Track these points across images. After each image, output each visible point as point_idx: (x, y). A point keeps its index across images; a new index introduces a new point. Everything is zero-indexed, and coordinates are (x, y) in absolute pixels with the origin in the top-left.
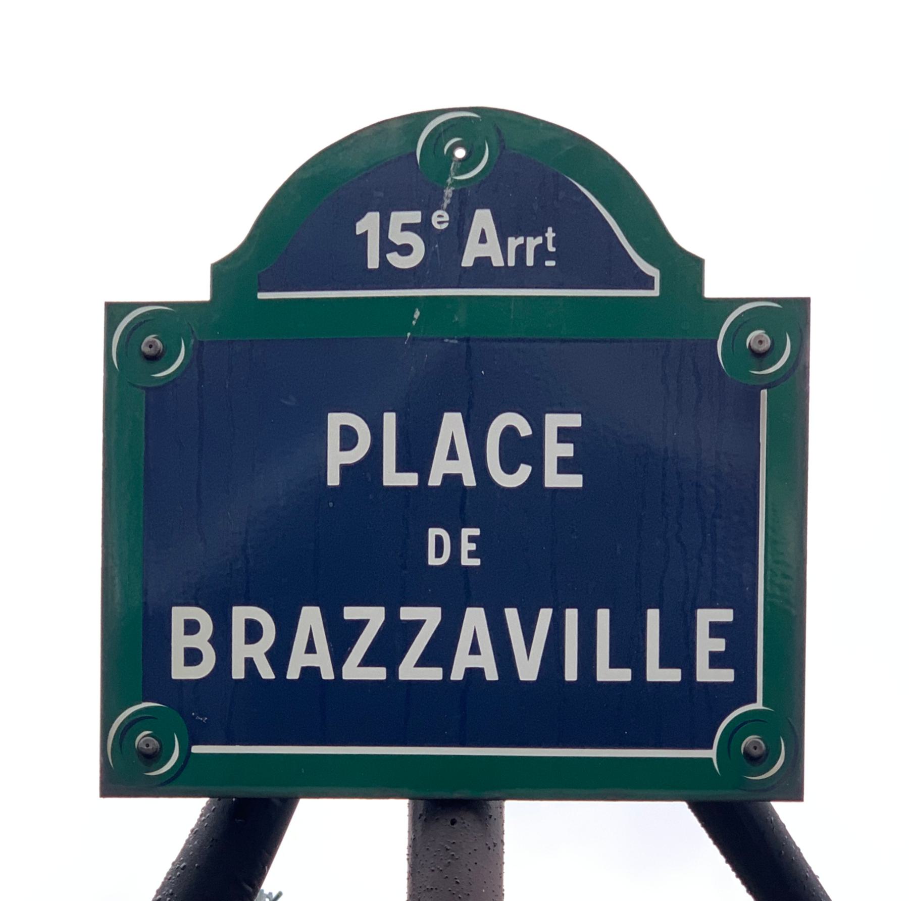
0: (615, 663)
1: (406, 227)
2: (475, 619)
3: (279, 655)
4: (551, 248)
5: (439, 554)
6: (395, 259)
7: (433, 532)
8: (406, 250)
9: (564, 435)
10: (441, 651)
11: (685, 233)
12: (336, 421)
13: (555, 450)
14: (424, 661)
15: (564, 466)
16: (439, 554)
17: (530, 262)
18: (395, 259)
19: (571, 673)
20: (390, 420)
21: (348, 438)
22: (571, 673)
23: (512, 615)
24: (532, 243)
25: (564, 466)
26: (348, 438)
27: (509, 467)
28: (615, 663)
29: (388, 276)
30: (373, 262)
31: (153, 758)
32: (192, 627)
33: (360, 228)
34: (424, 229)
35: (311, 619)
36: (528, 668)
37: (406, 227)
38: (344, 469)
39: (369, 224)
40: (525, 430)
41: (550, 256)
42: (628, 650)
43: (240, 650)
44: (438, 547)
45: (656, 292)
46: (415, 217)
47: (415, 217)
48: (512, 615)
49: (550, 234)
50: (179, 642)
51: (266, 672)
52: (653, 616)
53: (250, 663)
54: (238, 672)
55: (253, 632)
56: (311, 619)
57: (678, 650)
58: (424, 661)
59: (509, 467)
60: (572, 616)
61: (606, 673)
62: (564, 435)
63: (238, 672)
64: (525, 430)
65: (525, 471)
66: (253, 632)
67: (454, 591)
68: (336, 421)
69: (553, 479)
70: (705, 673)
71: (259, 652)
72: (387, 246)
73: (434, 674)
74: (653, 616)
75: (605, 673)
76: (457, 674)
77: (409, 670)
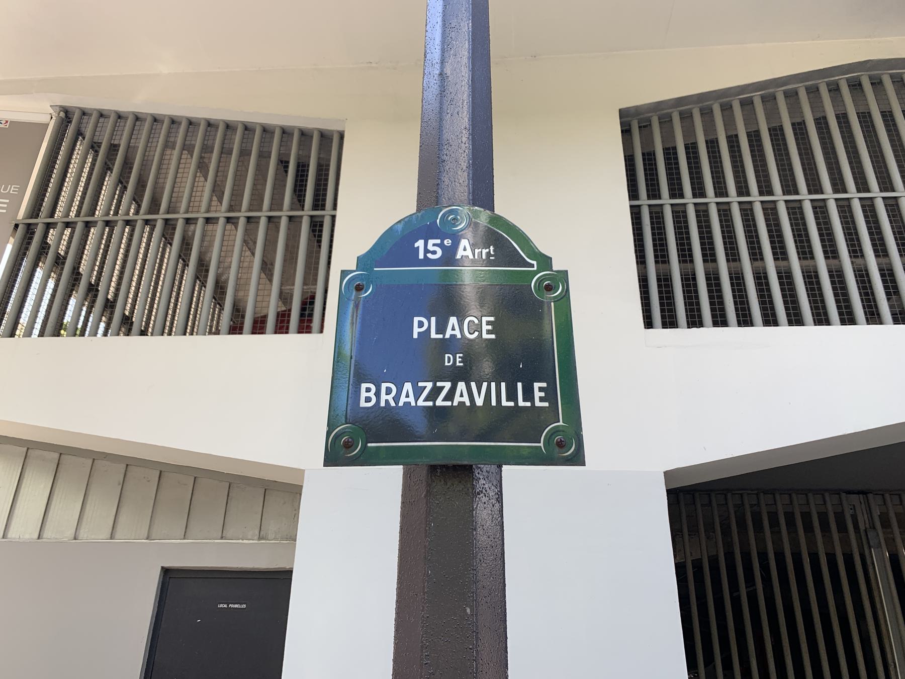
1: (434, 245)
3: (397, 399)
4: (492, 253)
6: (430, 255)
7: (447, 355)
8: (434, 253)
9: (488, 323)
10: (450, 396)
11: (543, 248)
12: (416, 320)
13: (485, 328)
14: (444, 400)
15: (489, 332)
17: (484, 257)
18: (430, 255)
19: (494, 403)
20: (433, 319)
21: (421, 324)
22: (494, 403)
23: (473, 384)
24: (485, 251)
25: (489, 332)
26: (421, 324)
29: (427, 262)
30: (421, 256)
31: (348, 446)
32: (368, 390)
33: (416, 245)
34: (441, 246)
35: (408, 386)
36: (479, 402)
37: (434, 245)
39: (420, 244)
40: (476, 321)
41: (492, 256)
42: (512, 396)
43: (384, 397)
44: (448, 360)
45: (535, 268)
46: (438, 241)
47: (438, 241)
48: (473, 384)
49: (492, 248)
50: (364, 394)
51: (393, 404)
52: (520, 385)
53: (387, 401)
54: (383, 404)
56: (408, 386)
57: (529, 394)
58: (444, 400)
60: (493, 385)
61: (505, 403)
62: (488, 323)
63: (383, 404)
64: (476, 321)
65: (476, 333)
67: (456, 375)
68: (416, 320)
70: (538, 403)
71: (390, 398)
72: (426, 251)
73: (449, 403)
74: (520, 385)
75: (505, 403)
76: (455, 404)
77: (439, 402)
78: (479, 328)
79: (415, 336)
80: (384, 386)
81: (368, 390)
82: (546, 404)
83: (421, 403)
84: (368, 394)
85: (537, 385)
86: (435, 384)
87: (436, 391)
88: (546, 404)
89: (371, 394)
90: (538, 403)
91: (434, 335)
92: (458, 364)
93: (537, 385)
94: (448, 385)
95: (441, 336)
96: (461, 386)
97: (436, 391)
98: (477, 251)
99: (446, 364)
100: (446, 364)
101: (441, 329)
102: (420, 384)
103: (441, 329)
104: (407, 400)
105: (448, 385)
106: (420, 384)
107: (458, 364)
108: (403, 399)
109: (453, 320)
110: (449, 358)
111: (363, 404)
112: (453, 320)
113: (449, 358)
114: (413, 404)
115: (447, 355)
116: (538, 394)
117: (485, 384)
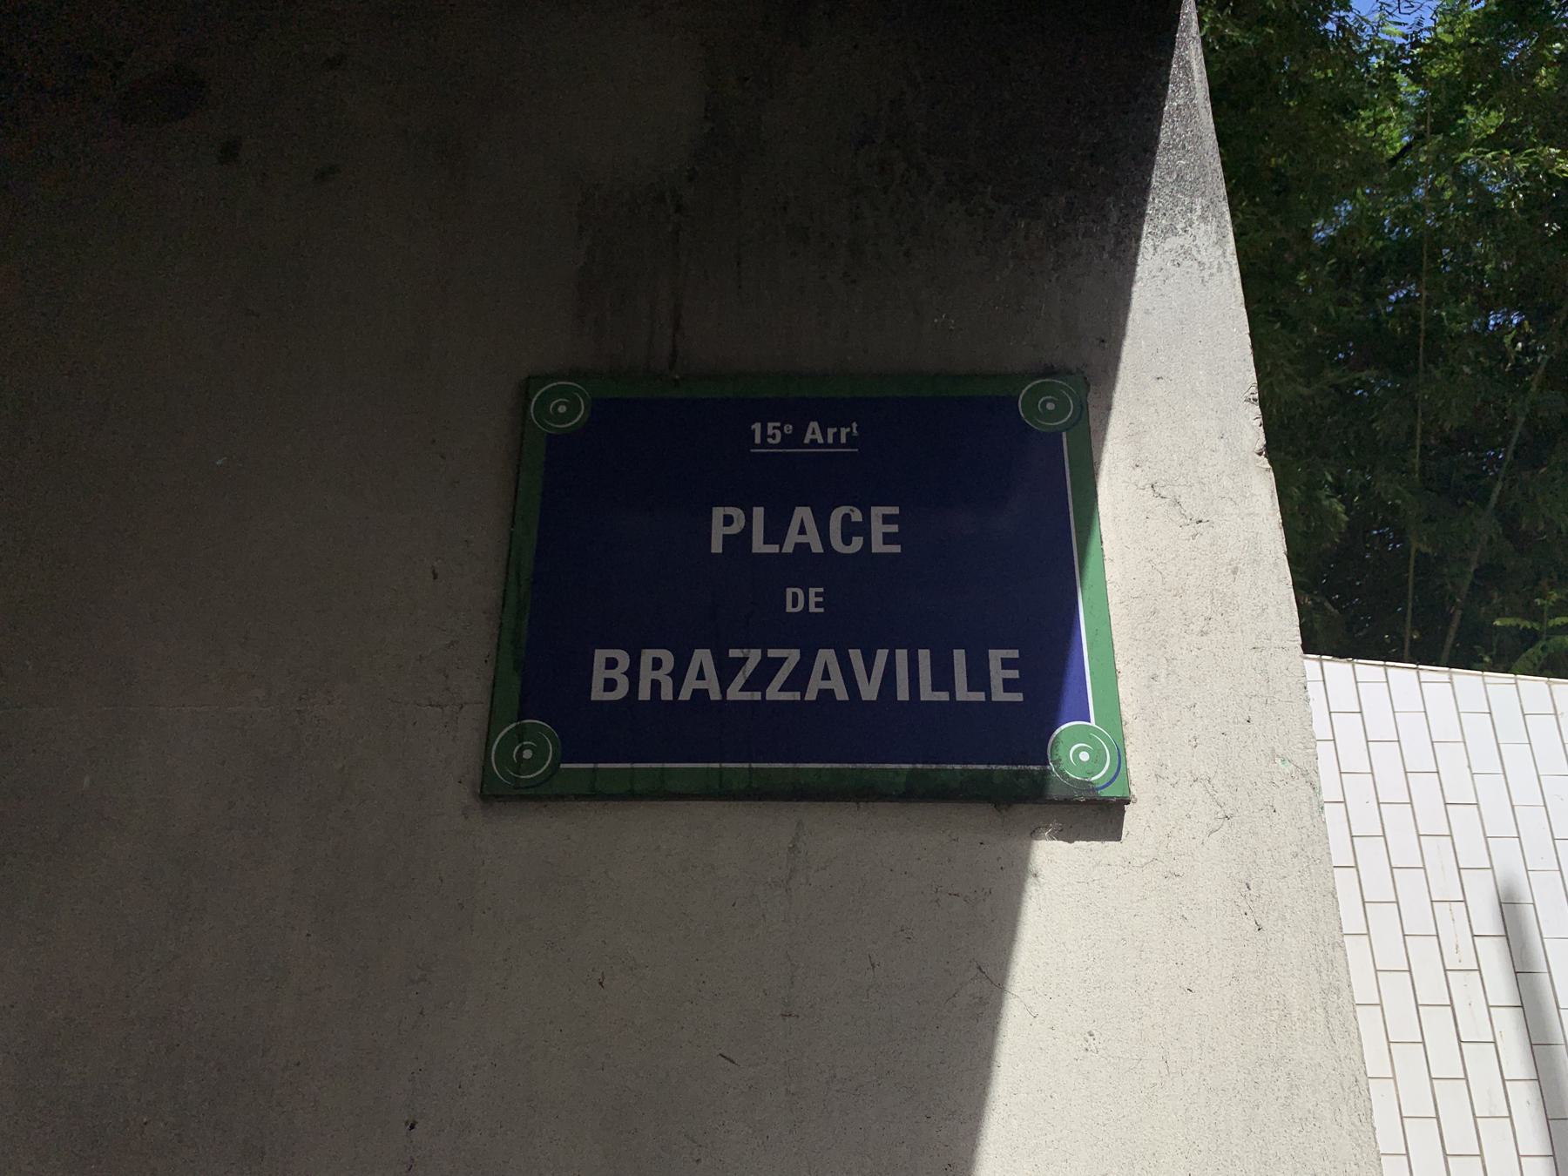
0: (936, 687)
2: (826, 656)
5: (794, 605)
7: (790, 591)
10: (799, 679)
13: (878, 529)
16: (794, 605)
26: (728, 521)
27: (847, 540)
28: (936, 687)
38: (727, 539)
40: (857, 516)
42: (943, 678)
50: (599, 674)
54: (644, 694)
55: (657, 664)
57: (978, 678)
59: (847, 540)
61: (927, 694)
63: (644, 694)
64: (857, 516)
65: (857, 543)
66: (657, 664)
69: (878, 547)
75: (927, 694)
76: (811, 695)
77: (774, 693)
78: (864, 529)
79: (717, 547)
80: (647, 656)
81: (611, 664)
82: (1018, 697)
83: (734, 693)
84: (611, 674)
85: (996, 656)
86: (764, 654)
87: (768, 668)
88: (1018, 697)
89: (617, 673)
90: (999, 695)
91: (759, 546)
92: (813, 609)
93: (996, 656)
94: (793, 656)
95: (774, 549)
96: (826, 656)
97: (768, 668)
98: (831, 431)
99: (789, 609)
100: (789, 609)
101: (775, 533)
102: (734, 653)
103: (775, 533)
104: (701, 685)
105: (793, 656)
106: (734, 653)
107: (813, 609)
108: (690, 684)
109: (803, 514)
110: (795, 596)
111: (598, 694)
112: (803, 514)
113: (795, 596)
114: (715, 695)
115: (790, 591)
116: (997, 674)
117: (882, 656)
